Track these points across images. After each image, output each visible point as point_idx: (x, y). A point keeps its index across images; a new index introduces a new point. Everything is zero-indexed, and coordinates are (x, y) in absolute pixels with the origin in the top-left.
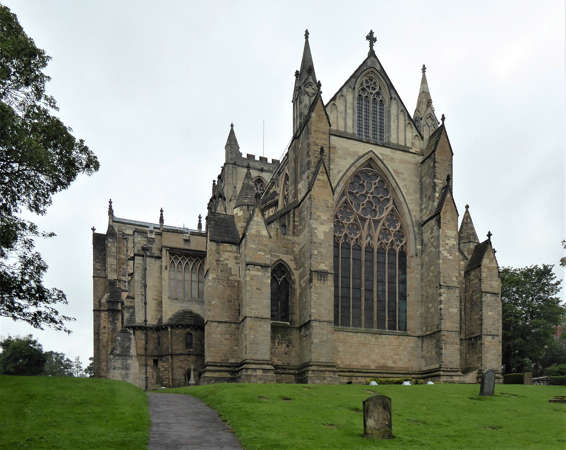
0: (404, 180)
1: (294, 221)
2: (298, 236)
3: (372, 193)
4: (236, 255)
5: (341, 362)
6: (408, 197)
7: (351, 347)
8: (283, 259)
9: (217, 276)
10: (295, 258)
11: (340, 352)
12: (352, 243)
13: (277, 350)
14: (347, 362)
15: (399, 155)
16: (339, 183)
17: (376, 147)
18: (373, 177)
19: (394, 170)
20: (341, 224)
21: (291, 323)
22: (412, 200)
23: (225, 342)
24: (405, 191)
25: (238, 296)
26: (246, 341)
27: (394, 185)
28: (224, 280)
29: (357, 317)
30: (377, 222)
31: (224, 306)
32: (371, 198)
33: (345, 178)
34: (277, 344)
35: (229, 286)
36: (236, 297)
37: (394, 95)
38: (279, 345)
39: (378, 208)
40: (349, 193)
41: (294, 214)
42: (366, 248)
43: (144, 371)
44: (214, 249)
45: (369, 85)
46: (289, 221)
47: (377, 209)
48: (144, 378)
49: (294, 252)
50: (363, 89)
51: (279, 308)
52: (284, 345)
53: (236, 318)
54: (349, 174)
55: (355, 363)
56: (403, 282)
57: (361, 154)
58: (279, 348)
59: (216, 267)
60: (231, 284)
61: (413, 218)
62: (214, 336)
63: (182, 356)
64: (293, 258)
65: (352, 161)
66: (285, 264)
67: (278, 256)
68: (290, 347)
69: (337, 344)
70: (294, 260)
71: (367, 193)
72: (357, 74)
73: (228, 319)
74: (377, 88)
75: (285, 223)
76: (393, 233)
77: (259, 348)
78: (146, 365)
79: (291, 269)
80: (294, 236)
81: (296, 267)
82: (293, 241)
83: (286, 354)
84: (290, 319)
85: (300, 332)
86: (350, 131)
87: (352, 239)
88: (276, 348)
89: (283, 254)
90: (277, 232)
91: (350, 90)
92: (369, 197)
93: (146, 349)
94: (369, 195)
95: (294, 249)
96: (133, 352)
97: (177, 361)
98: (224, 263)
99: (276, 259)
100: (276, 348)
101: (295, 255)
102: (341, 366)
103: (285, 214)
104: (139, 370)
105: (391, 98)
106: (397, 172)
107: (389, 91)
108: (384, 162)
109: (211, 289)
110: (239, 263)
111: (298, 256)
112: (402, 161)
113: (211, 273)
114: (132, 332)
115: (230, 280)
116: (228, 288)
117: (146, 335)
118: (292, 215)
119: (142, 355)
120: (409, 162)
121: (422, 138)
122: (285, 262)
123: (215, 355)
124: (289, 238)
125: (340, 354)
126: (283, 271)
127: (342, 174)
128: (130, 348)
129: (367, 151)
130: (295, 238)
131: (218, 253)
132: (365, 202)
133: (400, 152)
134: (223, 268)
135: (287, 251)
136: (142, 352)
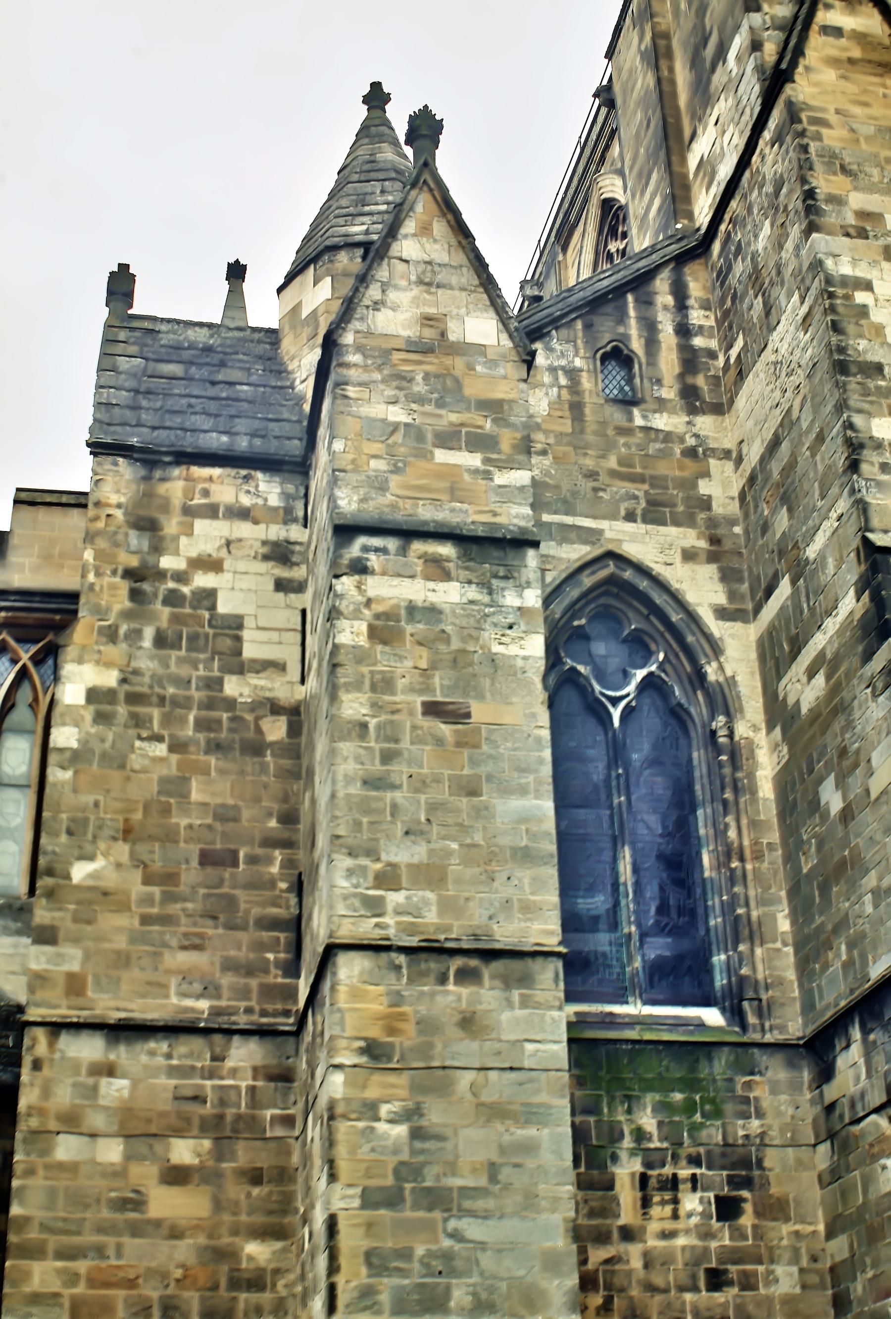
1: (684, 331)
2: (719, 409)
4: (276, 532)
8: (632, 550)
9: (124, 681)
10: (715, 540)
13: (634, 1253)
21: (736, 1014)
25: (289, 818)
26: (333, 1177)
31: (169, 898)
35: (215, 747)
36: (273, 823)
38: (646, 1203)
41: (680, 293)
44: (114, 499)
46: (650, 328)
49: (706, 503)
51: (628, 903)
52: (691, 1202)
53: (268, 992)
58: (654, 1227)
59: (127, 615)
60: (231, 730)
64: (703, 544)
66: (643, 584)
67: (591, 536)
68: (747, 1220)
70: (712, 558)
73: (204, 1005)
75: (625, 339)
77: (456, 1236)
79: (692, 617)
80: (692, 410)
81: (732, 596)
82: (691, 441)
84: (720, 981)
85: (825, 1073)
88: (628, 1234)
89: (630, 517)
95: (704, 487)
98: (186, 590)
100: (628, 1234)
101: (712, 523)
103: (618, 292)
109: (68, 774)
110: (299, 587)
111: (737, 530)
113: (80, 661)
115: (231, 704)
116: (213, 761)
118: (664, 297)
124: (661, 422)
130: (705, 423)
134: (175, 619)
135: (652, 503)
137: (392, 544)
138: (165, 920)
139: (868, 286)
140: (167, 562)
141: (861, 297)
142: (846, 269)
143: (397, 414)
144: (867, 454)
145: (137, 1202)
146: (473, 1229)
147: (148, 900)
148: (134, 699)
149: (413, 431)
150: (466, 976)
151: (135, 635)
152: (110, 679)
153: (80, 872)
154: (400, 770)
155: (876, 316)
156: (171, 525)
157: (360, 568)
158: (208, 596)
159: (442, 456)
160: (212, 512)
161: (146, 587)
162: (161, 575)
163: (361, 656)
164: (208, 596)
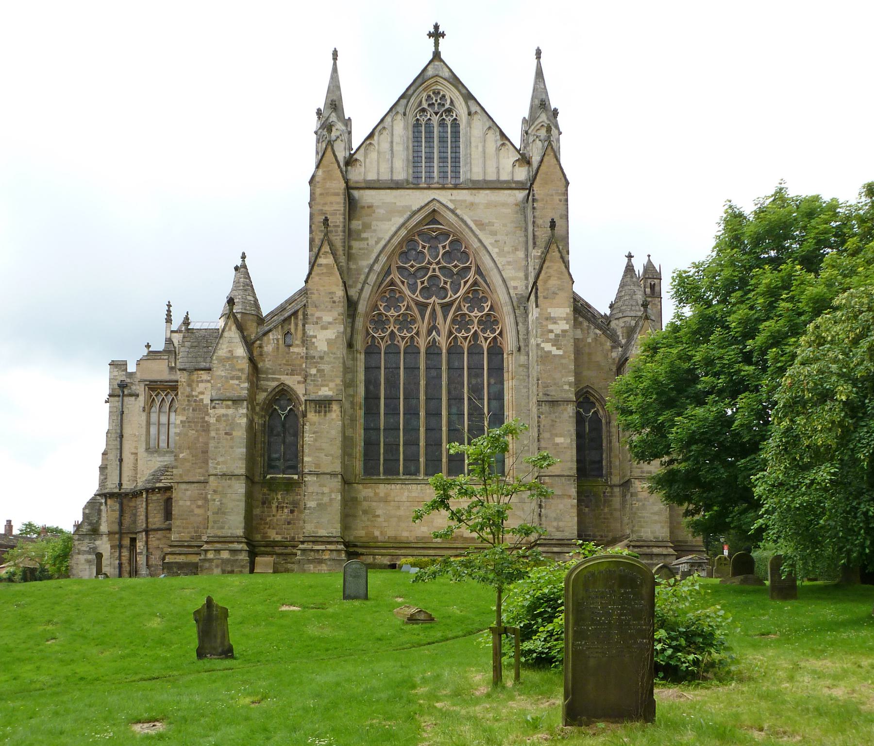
0: (494, 233)
3: (438, 263)
5: (381, 533)
6: (502, 259)
7: (399, 507)
8: (287, 382)
11: (378, 516)
12: (402, 345)
13: (275, 519)
14: (391, 533)
15: (483, 197)
16: (379, 255)
17: (443, 192)
18: (441, 238)
19: (475, 222)
20: (384, 318)
22: (509, 263)
23: (197, 511)
24: (496, 250)
27: (476, 244)
28: (197, 422)
29: (412, 459)
30: (446, 307)
32: (437, 269)
33: (390, 248)
34: (274, 509)
37: (474, 108)
38: (277, 511)
39: (449, 283)
40: (399, 268)
42: (428, 349)
43: (117, 554)
45: (434, 101)
46: (296, 325)
47: (448, 286)
48: (117, 565)
50: (424, 110)
54: (396, 241)
55: (405, 534)
56: (498, 397)
57: (415, 208)
58: (279, 514)
61: (511, 291)
62: (181, 503)
63: (159, 532)
65: (401, 220)
69: (374, 504)
71: (430, 263)
72: (410, 92)
74: (447, 106)
76: (476, 321)
78: (121, 546)
83: (289, 523)
86: (401, 175)
87: (403, 338)
89: (287, 374)
90: (278, 344)
91: (399, 117)
92: (434, 270)
93: (121, 524)
94: (434, 266)
96: (104, 528)
97: (154, 539)
99: (275, 384)
102: (380, 538)
103: (290, 317)
104: (111, 553)
105: (469, 114)
106: (481, 225)
107: (466, 103)
108: (458, 212)
112: (489, 205)
114: (103, 501)
117: (121, 505)
119: (115, 533)
120: (504, 205)
121: (529, 163)
122: (289, 386)
123: (181, 529)
125: (379, 520)
126: (289, 400)
127: (383, 243)
128: (100, 525)
129: (426, 202)
131: (189, 385)
132: (426, 278)
133: (488, 192)
136: (116, 528)
137: (220, 402)
138: (195, 463)
139: (315, 337)
140: (194, 393)
141: (314, 340)
142: (311, 333)
143: (223, 374)
144: (309, 378)
145: (192, 511)
146: (229, 517)
147: (193, 460)
148: (189, 422)
149: (226, 377)
150: (230, 479)
151: (188, 409)
152: (184, 418)
153: (181, 456)
154: (220, 444)
155: (316, 344)
156: (194, 385)
157: (214, 408)
158: (202, 400)
159: (231, 382)
160: (202, 381)
161: (190, 399)
162: (193, 396)
163: (214, 425)
164: (202, 400)
